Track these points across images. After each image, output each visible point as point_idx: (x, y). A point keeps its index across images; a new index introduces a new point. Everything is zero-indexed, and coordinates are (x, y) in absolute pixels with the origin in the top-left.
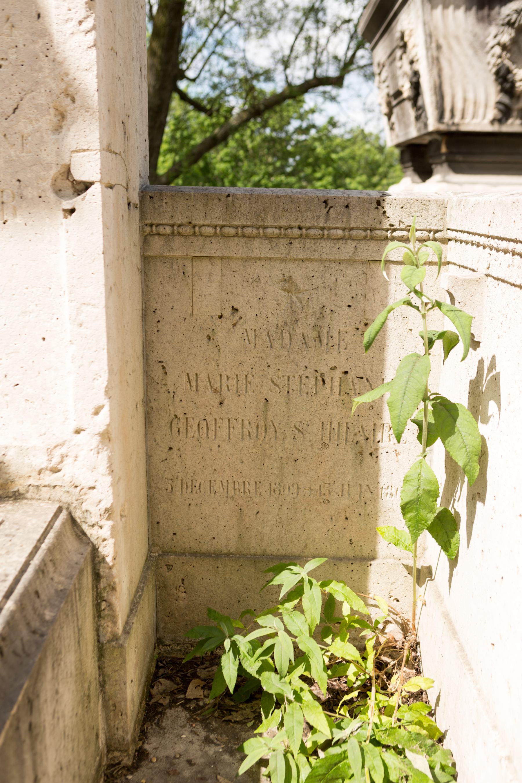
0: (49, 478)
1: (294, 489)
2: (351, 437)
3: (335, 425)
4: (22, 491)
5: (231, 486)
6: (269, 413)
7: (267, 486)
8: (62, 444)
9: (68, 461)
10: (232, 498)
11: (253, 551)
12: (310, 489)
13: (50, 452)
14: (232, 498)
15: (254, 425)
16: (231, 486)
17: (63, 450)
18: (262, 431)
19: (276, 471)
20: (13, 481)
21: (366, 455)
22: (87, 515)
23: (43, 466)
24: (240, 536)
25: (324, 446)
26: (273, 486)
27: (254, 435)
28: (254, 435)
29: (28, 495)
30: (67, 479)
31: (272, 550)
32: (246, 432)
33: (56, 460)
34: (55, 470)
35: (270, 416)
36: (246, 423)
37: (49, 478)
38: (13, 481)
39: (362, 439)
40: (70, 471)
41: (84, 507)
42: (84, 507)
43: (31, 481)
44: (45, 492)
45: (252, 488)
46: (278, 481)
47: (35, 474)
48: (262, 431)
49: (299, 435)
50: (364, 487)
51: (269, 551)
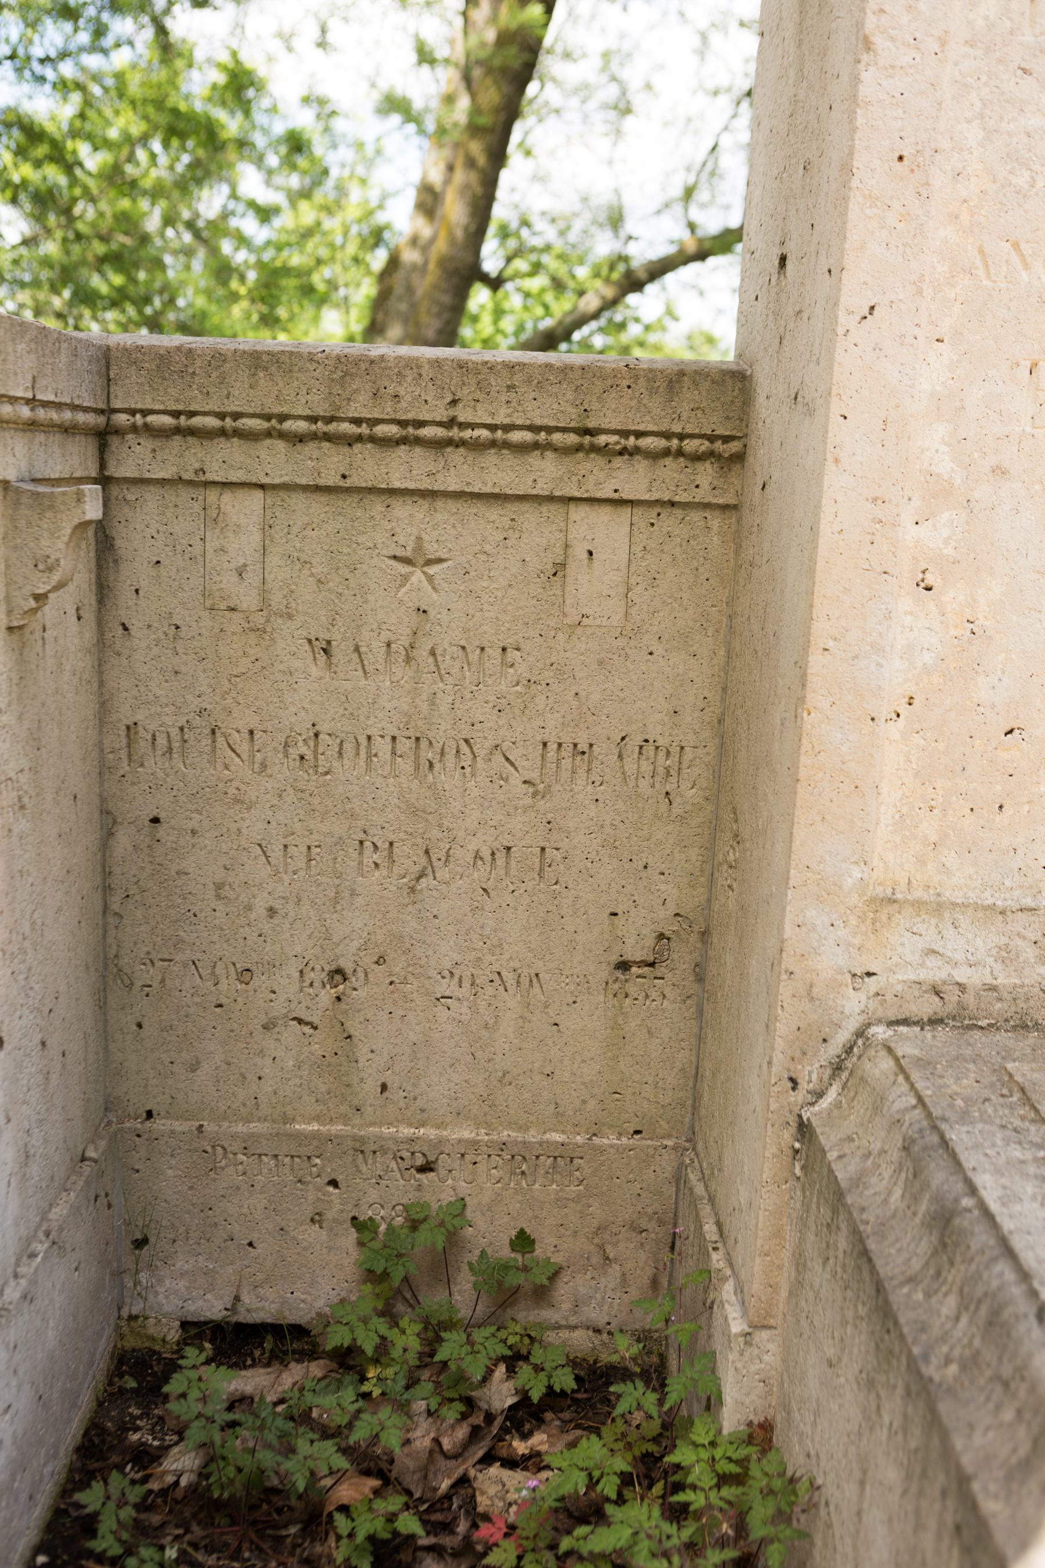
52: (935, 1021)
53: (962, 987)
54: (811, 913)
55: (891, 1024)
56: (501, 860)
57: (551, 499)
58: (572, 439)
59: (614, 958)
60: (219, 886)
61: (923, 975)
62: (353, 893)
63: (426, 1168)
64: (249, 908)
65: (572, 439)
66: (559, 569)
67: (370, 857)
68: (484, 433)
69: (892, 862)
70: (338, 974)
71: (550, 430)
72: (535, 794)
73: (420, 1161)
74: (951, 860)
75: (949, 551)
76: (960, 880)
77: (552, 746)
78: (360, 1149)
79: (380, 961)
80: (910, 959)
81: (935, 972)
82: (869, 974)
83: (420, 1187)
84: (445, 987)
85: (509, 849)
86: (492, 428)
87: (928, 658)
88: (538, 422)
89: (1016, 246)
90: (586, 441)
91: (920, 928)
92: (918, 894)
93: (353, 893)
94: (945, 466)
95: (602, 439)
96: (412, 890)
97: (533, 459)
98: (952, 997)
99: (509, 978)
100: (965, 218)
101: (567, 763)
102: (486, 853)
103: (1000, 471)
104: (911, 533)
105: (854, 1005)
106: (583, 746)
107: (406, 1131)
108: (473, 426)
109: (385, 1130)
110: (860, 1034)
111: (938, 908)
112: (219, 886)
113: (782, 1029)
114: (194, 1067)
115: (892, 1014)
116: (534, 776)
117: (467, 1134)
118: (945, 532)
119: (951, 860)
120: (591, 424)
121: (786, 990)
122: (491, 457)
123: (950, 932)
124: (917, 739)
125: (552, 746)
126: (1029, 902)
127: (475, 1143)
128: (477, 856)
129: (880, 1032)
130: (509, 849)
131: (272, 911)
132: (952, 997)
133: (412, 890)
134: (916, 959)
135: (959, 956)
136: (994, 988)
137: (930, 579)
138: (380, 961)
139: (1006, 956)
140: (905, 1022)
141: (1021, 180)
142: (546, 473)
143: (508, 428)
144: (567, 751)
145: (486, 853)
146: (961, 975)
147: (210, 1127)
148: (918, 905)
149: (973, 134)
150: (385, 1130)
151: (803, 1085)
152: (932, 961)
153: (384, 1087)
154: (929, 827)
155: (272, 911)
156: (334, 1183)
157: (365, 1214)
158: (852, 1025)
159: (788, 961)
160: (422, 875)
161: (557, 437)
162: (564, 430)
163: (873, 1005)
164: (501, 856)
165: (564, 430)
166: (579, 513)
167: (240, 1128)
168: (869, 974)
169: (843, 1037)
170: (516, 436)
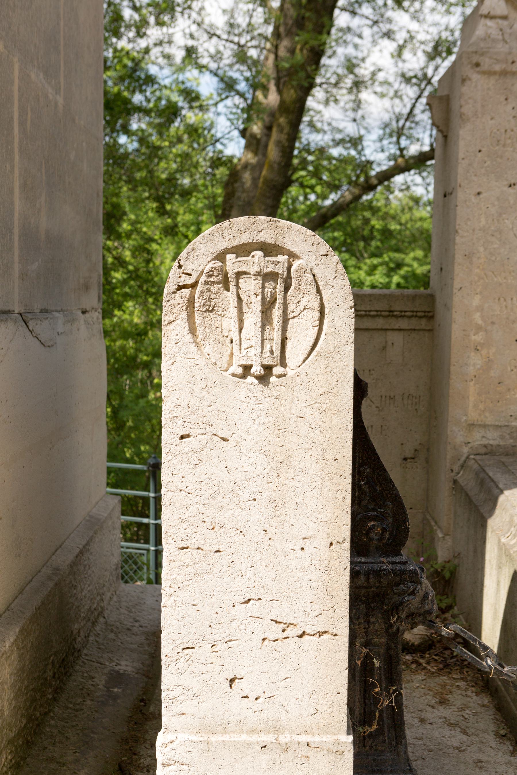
52: (486, 454)
53: (492, 445)
54: (454, 428)
55: (475, 455)
57: (381, 329)
58: (387, 313)
59: (403, 457)
61: (482, 443)
65: (387, 313)
66: (384, 348)
68: (363, 313)
69: (473, 415)
71: (381, 311)
72: (379, 410)
74: (487, 414)
75: (482, 341)
76: (490, 419)
77: (384, 397)
80: (478, 438)
81: (485, 442)
82: (469, 443)
85: (372, 426)
86: (365, 311)
87: (479, 366)
88: (378, 309)
89: (493, 272)
90: (391, 314)
91: (481, 431)
92: (480, 423)
94: (480, 322)
95: (395, 313)
97: (377, 319)
98: (489, 448)
100: (481, 267)
101: (388, 402)
103: (493, 323)
104: (473, 338)
105: (465, 450)
106: (392, 397)
108: (360, 311)
110: (468, 457)
111: (485, 426)
113: (448, 457)
116: (379, 405)
118: (481, 337)
119: (487, 414)
120: (392, 309)
121: (449, 447)
122: (365, 319)
123: (488, 432)
124: (477, 386)
125: (384, 397)
126: (507, 424)
129: (472, 457)
130: (372, 426)
135: (490, 438)
136: (499, 446)
137: (478, 348)
139: (502, 437)
140: (478, 454)
141: (493, 258)
142: (380, 323)
143: (370, 311)
144: (388, 398)
146: (491, 442)
148: (480, 426)
149: (482, 249)
151: (455, 471)
152: (484, 439)
154: (481, 407)
158: (465, 456)
161: (383, 313)
162: (385, 311)
165: (385, 311)
166: (389, 333)
168: (469, 443)
169: (463, 459)
170: (372, 313)
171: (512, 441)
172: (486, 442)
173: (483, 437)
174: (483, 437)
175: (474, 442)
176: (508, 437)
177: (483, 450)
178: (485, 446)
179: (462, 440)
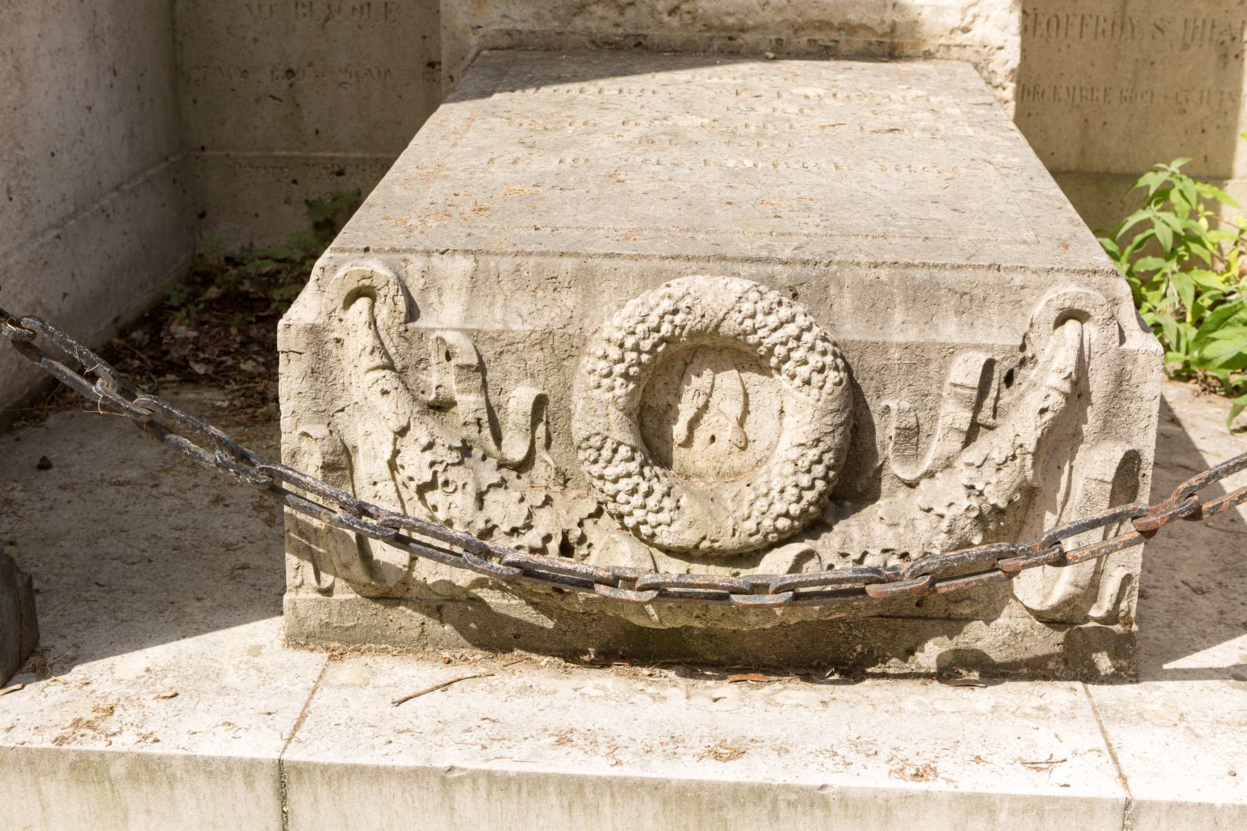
0: (960, 38)
1: (1147, 97)
2: (1216, 37)
3: (1199, 23)
4: (932, 50)
5: (1078, 93)
6: (1128, 8)
7: (1118, 94)
8: (975, 4)
9: (979, 21)
10: (1078, 107)
11: (1095, 169)
12: (1166, 97)
13: (964, 11)
14: (1078, 107)
15: (1109, 22)
16: (1078, 93)
17: (975, 10)
18: (1118, 28)
19: (1129, 76)
20: (924, 41)
21: (1231, 57)
22: (993, 76)
23: (956, 25)
24: (1083, 152)
25: (1186, 47)
26: (1125, 93)
27: (1108, 33)
28: (1108, 33)
29: (938, 55)
30: (977, 38)
31: (1116, 168)
32: (1100, 30)
33: (968, 19)
34: (966, 30)
35: (1129, 9)
36: (1101, 19)
37: (960, 38)
38: (924, 41)
39: (1227, 39)
40: (980, 31)
41: (991, 67)
42: (991, 67)
43: (943, 41)
44: (955, 52)
45: (1101, 95)
46: (1131, 87)
47: (947, 33)
48: (1118, 28)
49: (1158, 34)
50: (1226, 95)
51: (1113, 169)
52: (509, 48)
53: (520, 32)
55: (491, 49)
56: (366, 11)
59: (426, 60)
60: (229, 28)
61: (502, 26)
62: (295, 30)
63: (340, 173)
64: (244, 38)
67: (301, 11)
70: (290, 72)
73: (336, 169)
78: (307, 163)
79: (310, 64)
81: (507, 25)
83: (338, 183)
84: (342, 78)
85: (369, 4)
93: (295, 30)
96: (323, 27)
98: (516, 36)
99: (375, 72)
102: (358, 6)
105: (474, 40)
107: (329, 154)
109: (319, 154)
110: (477, 54)
112: (229, 28)
114: (223, 123)
115: (491, 45)
117: (360, 155)
121: (444, 35)
123: (512, 7)
127: (362, 159)
128: (354, 9)
129: (485, 52)
130: (369, 4)
131: (255, 40)
132: (516, 36)
133: (323, 27)
134: (499, 19)
135: (517, 18)
136: (533, 32)
138: (310, 64)
139: (538, 17)
140: (496, 49)
145: (358, 6)
146: (519, 26)
147: (232, 153)
150: (319, 154)
152: (506, 21)
153: (317, 132)
155: (255, 40)
156: (295, 182)
157: (313, 198)
158: (474, 51)
159: (443, 22)
160: (327, 20)
163: (482, 41)
164: (365, 7)
167: (248, 154)
169: (470, 56)
171: (556, 24)
172: (511, 26)
173: (505, 16)
174: (505, 16)
175: (488, 25)
176: (549, 16)
177: (505, 41)
178: (509, 33)
179: (466, 21)
